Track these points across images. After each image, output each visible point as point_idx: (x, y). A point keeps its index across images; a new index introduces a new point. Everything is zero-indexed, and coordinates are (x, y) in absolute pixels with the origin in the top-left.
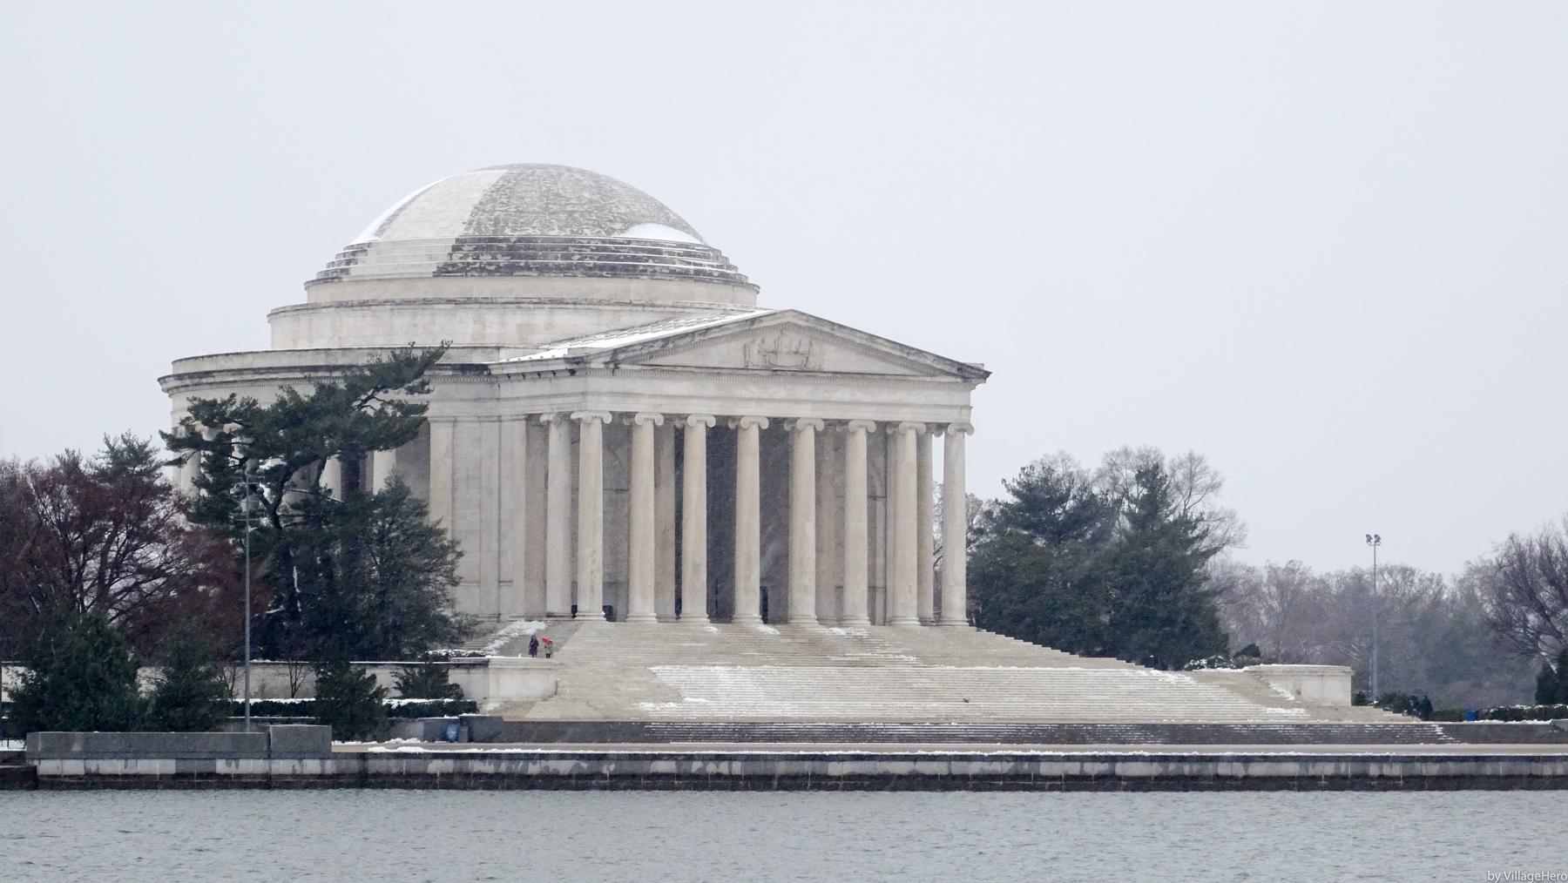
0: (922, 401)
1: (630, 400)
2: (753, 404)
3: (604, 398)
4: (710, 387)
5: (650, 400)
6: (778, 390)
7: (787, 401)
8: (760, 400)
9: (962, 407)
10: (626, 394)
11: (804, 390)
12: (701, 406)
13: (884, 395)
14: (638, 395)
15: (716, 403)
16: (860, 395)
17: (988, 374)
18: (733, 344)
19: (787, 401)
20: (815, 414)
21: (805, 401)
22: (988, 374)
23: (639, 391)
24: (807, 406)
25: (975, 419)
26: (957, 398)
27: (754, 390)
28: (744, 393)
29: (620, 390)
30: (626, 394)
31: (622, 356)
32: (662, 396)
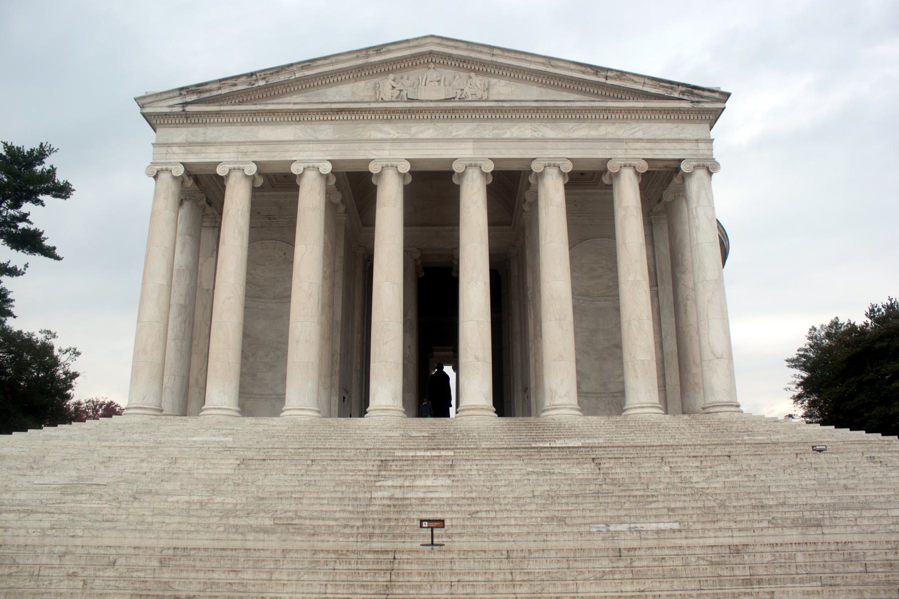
0: (639, 135)
1: (212, 149)
2: (388, 146)
3: (175, 149)
4: (326, 131)
5: (236, 152)
6: (426, 130)
7: (435, 140)
8: (394, 141)
9: (697, 141)
10: (204, 144)
11: (462, 129)
12: (311, 153)
13: (582, 130)
14: (222, 144)
15: (333, 147)
16: (548, 131)
17: (728, 95)
18: (361, 84)
19: (435, 140)
20: (479, 154)
21: (463, 140)
22: (728, 95)
23: (224, 139)
24: (470, 151)
25: (717, 155)
26: (691, 131)
27: (391, 131)
29: (200, 139)
30: (204, 144)
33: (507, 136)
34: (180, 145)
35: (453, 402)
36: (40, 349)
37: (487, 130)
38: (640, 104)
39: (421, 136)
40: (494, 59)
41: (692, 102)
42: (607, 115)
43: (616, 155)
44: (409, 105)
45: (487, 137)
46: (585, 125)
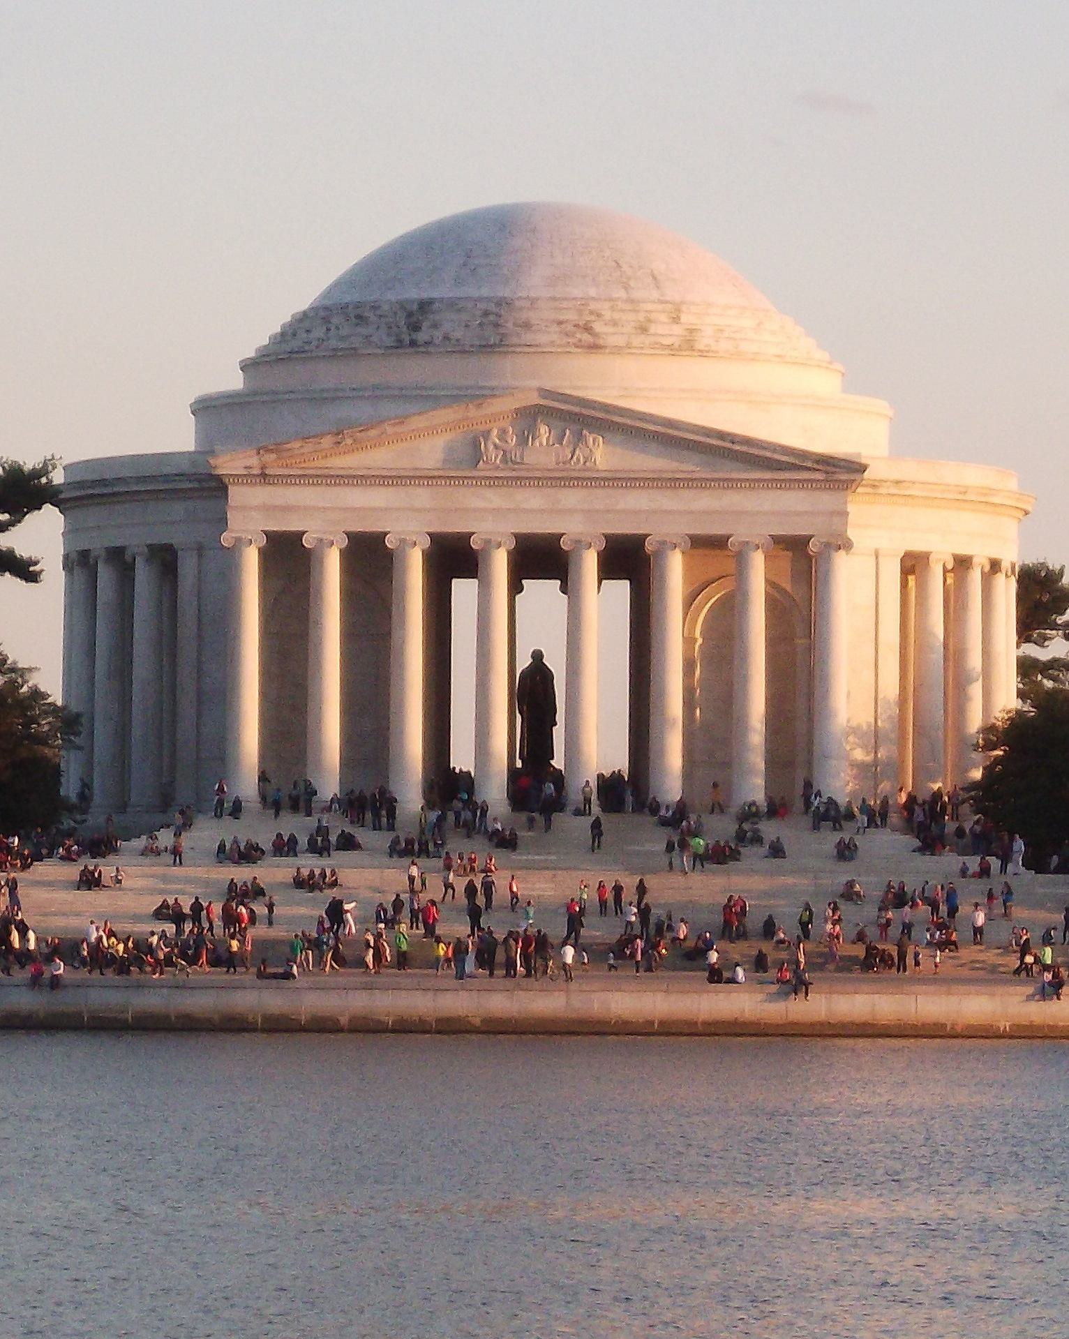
4: (421, 496)
6: (532, 499)
8: (496, 511)
9: (832, 513)
11: (571, 498)
13: (704, 501)
14: (306, 508)
19: (542, 511)
26: (825, 500)
27: (493, 498)
28: (477, 503)
31: (273, 456)
32: (345, 509)
33: (621, 506)
34: (257, 508)
35: (560, 717)
36: (22, 701)
37: (599, 498)
38: (768, 475)
39: (525, 506)
40: (608, 417)
41: (827, 473)
42: (729, 484)
43: (740, 532)
44: (514, 474)
45: (597, 507)
46: (707, 492)
